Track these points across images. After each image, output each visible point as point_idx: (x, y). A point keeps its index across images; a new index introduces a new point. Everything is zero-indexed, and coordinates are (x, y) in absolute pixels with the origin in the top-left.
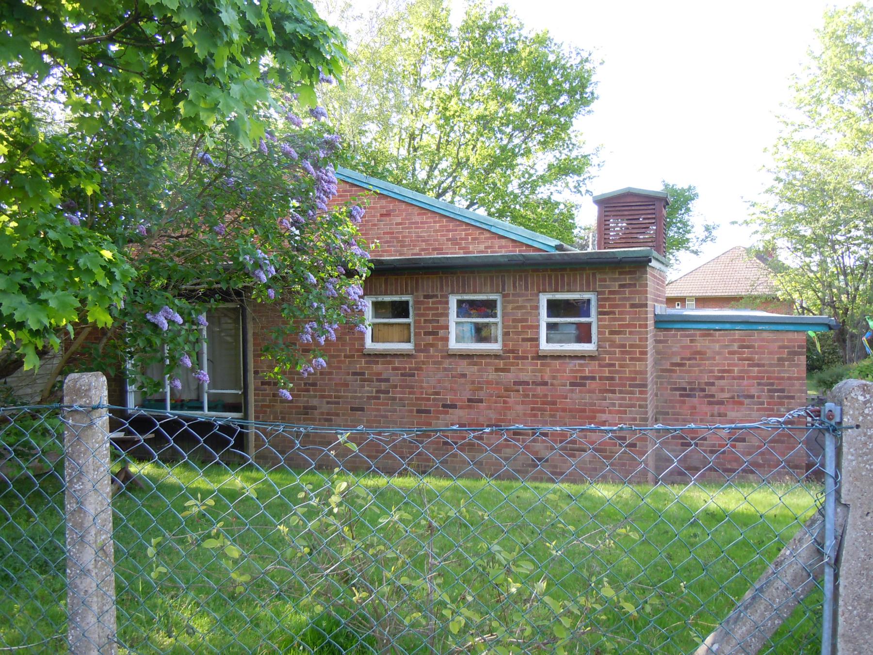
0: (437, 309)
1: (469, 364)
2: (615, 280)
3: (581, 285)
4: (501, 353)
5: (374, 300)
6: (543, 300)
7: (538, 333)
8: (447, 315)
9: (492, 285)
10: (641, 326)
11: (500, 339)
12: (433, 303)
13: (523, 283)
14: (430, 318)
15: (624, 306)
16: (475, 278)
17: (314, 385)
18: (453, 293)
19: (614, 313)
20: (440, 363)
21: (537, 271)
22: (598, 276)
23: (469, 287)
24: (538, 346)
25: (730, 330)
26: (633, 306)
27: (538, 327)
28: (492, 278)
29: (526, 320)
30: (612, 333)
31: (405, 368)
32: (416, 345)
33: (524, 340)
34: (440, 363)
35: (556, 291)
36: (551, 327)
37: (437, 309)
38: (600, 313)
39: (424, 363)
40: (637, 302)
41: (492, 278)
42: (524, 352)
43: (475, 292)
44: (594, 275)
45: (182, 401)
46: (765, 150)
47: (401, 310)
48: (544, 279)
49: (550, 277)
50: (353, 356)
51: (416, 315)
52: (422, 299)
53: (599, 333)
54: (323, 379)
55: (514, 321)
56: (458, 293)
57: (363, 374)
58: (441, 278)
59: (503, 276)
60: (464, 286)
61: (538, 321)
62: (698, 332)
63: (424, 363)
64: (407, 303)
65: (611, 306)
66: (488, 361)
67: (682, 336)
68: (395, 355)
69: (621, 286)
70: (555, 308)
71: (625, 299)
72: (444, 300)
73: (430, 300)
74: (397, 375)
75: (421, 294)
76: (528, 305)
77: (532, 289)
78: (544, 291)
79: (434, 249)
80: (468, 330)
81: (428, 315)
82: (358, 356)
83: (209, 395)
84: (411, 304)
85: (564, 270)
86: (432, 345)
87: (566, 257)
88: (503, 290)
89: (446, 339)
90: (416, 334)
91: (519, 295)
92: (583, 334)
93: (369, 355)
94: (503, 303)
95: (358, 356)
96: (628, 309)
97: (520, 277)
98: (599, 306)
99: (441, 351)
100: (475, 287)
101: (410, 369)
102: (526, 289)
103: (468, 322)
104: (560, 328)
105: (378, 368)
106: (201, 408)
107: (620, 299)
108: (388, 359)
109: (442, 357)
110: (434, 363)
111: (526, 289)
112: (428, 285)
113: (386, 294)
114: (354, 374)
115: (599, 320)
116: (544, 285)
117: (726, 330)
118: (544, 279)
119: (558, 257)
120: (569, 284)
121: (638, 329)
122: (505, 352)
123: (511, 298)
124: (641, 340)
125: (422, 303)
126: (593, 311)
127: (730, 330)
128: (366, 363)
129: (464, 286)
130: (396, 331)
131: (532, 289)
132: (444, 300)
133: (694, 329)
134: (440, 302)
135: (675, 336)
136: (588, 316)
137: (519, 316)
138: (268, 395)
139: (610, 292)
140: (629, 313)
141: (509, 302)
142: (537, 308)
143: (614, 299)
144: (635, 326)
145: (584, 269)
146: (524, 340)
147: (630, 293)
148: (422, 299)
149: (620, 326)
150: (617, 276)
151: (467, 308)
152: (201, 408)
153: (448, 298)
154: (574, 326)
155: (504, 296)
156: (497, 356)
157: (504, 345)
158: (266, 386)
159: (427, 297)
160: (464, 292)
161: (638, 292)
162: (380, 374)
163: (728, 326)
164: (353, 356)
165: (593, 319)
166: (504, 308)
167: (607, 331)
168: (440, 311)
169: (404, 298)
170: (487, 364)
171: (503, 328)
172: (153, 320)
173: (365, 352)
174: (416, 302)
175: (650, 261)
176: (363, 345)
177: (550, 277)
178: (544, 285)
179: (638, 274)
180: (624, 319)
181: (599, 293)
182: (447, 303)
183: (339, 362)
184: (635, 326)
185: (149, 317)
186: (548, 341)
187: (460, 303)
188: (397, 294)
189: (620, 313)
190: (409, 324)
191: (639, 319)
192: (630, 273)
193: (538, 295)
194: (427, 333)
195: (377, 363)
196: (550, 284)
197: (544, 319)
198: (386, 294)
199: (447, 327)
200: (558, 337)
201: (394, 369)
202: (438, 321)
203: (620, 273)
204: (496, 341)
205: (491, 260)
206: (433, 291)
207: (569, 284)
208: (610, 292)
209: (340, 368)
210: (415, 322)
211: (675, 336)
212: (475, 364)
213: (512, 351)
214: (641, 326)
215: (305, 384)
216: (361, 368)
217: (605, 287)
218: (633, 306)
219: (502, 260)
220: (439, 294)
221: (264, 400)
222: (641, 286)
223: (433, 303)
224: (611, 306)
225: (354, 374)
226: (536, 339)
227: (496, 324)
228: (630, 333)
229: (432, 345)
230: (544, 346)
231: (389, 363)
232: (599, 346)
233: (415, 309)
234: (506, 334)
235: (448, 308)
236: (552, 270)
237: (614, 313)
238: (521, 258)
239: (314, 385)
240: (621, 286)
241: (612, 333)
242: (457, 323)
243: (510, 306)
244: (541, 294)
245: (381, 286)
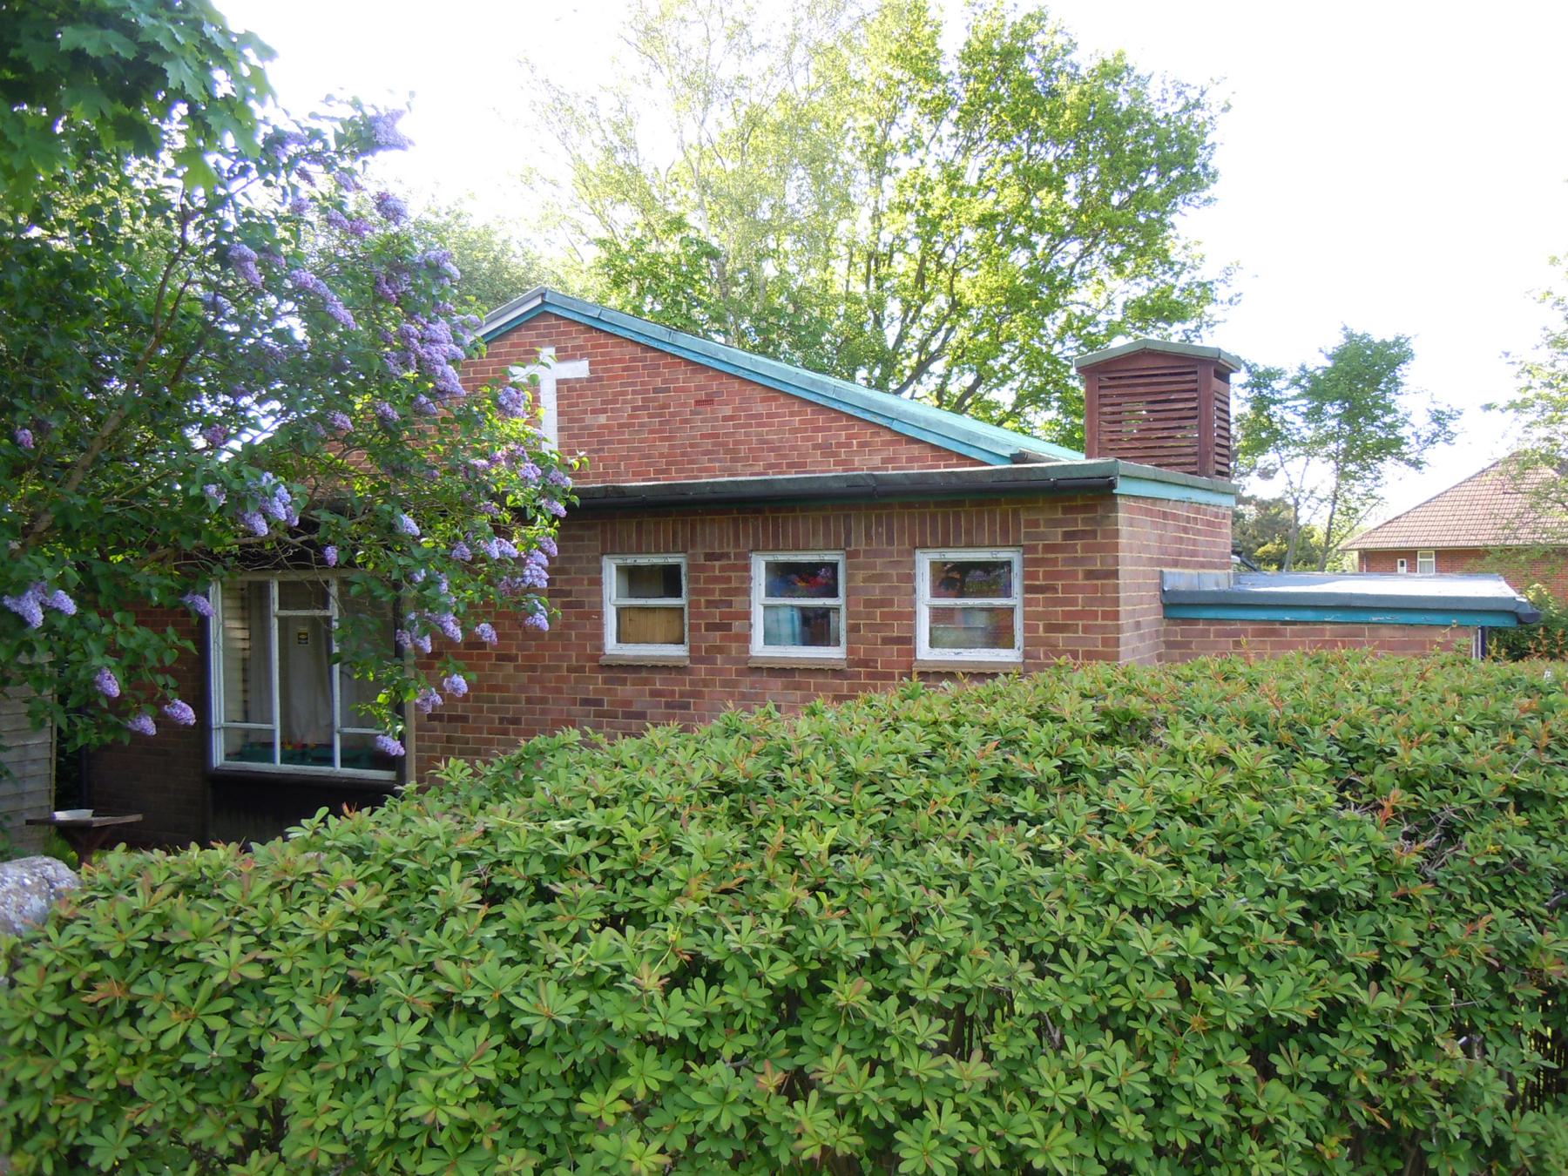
0: (729, 579)
1: (786, 687)
2: (1055, 523)
3: (992, 533)
4: (844, 665)
5: (620, 562)
6: (759, 567)
7: (912, 628)
8: (747, 592)
9: (827, 534)
10: (1105, 615)
11: (843, 639)
12: (722, 569)
13: (883, 530)
14: (717, 597)
15: (1074, 575)
16: (795, 519)
17: (516, 721)
18: (756, 549)
19: (1054, 589)
20: (734, 684)
21: (909, 506)
22: (1023, 517)
23: (785, 537)
24: (913, 652)
25: (1315, 623)
26: (1090, 575)
27: (912, 615)
28: (826, 520)
29: (890, 603)
30: (1050, 628)
31: (673, 692)
32: (691, 649)
33: (886, 641)
34: (734, 684)
35: (946, 545)
36: (938, 615)
37: (729, 579)
38: (1028, 589)
39: (705, 683)
40: (1099, 567)
41: (826, 520)
42: (886, 664)
43: (796, 548)
44: (1016, 513)
45: (305, 746)
46: (472, 196)
47: (669, 580)
48: (923, 523)
49: (934, 518)
50: (581, 669)
51: (692, 591)
52: (702, 561)
53: (1027, 628)
54: (532, 712)
55: (868, 603)
56: (766, 549)
57: (599, 703)
58: (735, 521)
59: (847, 517)
60: (776, 537)
61: (913, 604)
62: (1250, 628)
63: (705, 683)
64: (677, 568)
65: (1048, 575)
66: (821, 680)
67: (1218, 634)
68: (655, 668)
69: (1068, 535)
70: (952, 579)
71: (1076, 561)
72: (743, 562)
73: (717, 563)
74: (658, 705)
75: (700, 551)
76: (894, 572)
77: (901, 542)
78: (924, 546)
79: (701, 470)
80: (789, 623)
81: (712, 592)
82: (592, 670)
83: (344, 737)
84: (684, 570)
85: (959, 503)
86: (720, 650)
87: (954, 480)
88: (848, 543)
89: (746, 639)
90: (693, 628)
91: (876, 554)
92: (999, 635)
93: (609, 667)
94: (849, 567)
95: (592, 670)
96: (1081, 582)
97: (879, 518)
98: (1027, 575)
99: (737, 661)
100: (796, 537)
101: (682, 694)
102: (890, 541)
103: (786, 606)
104: (958, 617)
105: (626, 691)
106: (329, 761)
107: (1066, 561)
108: (644, 675)
109: (740, 673)
110: (725, 684)
111: (890, 541)
112: (713, 535)
113: (639, 552)
114: (586, 702)
115: (1027, 603)
116: (923, 533)
117: (1306, 623)
118: (923, 523)
119: (938, 478)
120: (968, 532)
121: (1100, 622)
122: (853, 663)
123: (861, 559)
124: (1105, 642)
125: (702, 568)
126: (1017, 585)
127: (1315, 623)
128: (605, 681)
129: (776, 537)
130: (659, 621)
131: (901, 542)
132: (743, 562)
133: (1242, 621)
134: (734, 568)
135: (1205, 633)
136: (1008, 594)
137: (877, 594)
138: (438, 739)
139: (1048, 548)
140: (1082, 589)
141: (858, 567)
142: (910, 578)
143: (1054, 562)
144: (1094, 615)
145: (997, 502)
146: (886, 641)
147: (1086, 548)
148: (702, 561)
149: (1067, 615)
150: (1060, 516)
151: (786, 578)
152: (329, 761)
153: (747, 558)
154: (984, 614)
155: (851, 555)
156: (836, 673)
157: (850, 651)
158: (436, 723)
159: (710, 557)
160: (776, 549)
161: (1101, 548)
162: (628, 703)
163: (1309, 615)
164: (581, 669)
165: (1016, 600)
166: (849, 578)
167: (1041, 624)
168: (733, 585)
169: (672, 560)
170: (819, 688)
171: (848, 617)
172: (15, 609)
173: (603, 661)
174: (693, 568)
175: (1112, 485)
176: (600, 647)
177: (934, 518)
178: (923, 533)
179: (1100, 511)
180: (1073, 602)
181: (1028, 549)
182: (747, 568)
183: (560, 679)
184: (1094, 615)
185: (8, 601)
186: (933, 643)
187: (775, 569)
188: (658, 552)
189: (1066, 589)
190: (682, 609)
191: (1103, 601)
192: (1085, 508)
193: (911, 553)
194: (711, 627)
195: (623, 682)
196: (934, 533)
197: (925, 599)
198: (639, 551)
199: (746, 616)
200: (953, 636)
201: (654, 693)
202: (730, 604)
203: (1066, 510)
204: (838, 643)
205: (815, 485)
206: (721, 546)
207: (968, 532)
208: (1048, 548)
209: (558, 691)
210: (691, 605)
211: (1205, 633)
212: (798, 687)
213: (865, 663)
214: (1105, 615)
215: (502, 720)
216: (596, 691)
217: (1037, 536)
218: (1090, 575)
219: (835, 485)
220: (732, 551)
221: (432, 749)
222: (1105, 535)
223: (722, 569)
224: (1048, 575)
225: (586, 702)
226: (908, 641)
227: (837, 609)
228: (1086, 629)
229: (720, 650)
230: (925, 652)
231: (646, 682)
232: (1026, 655)
233: (690, 581)
234: (853, 629)
235: (750, 579)
236: (937, 505)
237: (1054, 589)
238: (872, 483)
239: (516, 721)
240: (1068, 535)
241: (1050, 628)
242: (766, 607)
243: (861, 574)
244: (918, 552)
245: (629, 537)
